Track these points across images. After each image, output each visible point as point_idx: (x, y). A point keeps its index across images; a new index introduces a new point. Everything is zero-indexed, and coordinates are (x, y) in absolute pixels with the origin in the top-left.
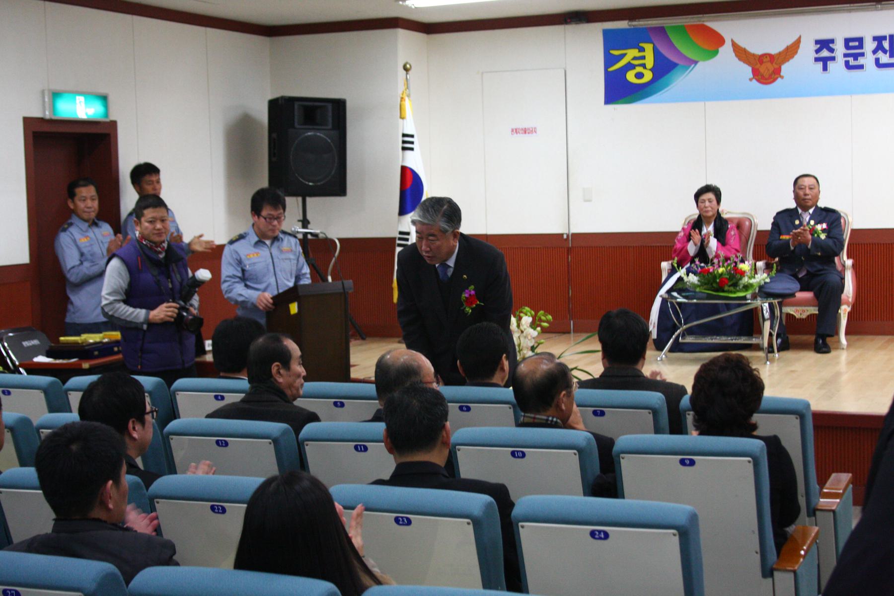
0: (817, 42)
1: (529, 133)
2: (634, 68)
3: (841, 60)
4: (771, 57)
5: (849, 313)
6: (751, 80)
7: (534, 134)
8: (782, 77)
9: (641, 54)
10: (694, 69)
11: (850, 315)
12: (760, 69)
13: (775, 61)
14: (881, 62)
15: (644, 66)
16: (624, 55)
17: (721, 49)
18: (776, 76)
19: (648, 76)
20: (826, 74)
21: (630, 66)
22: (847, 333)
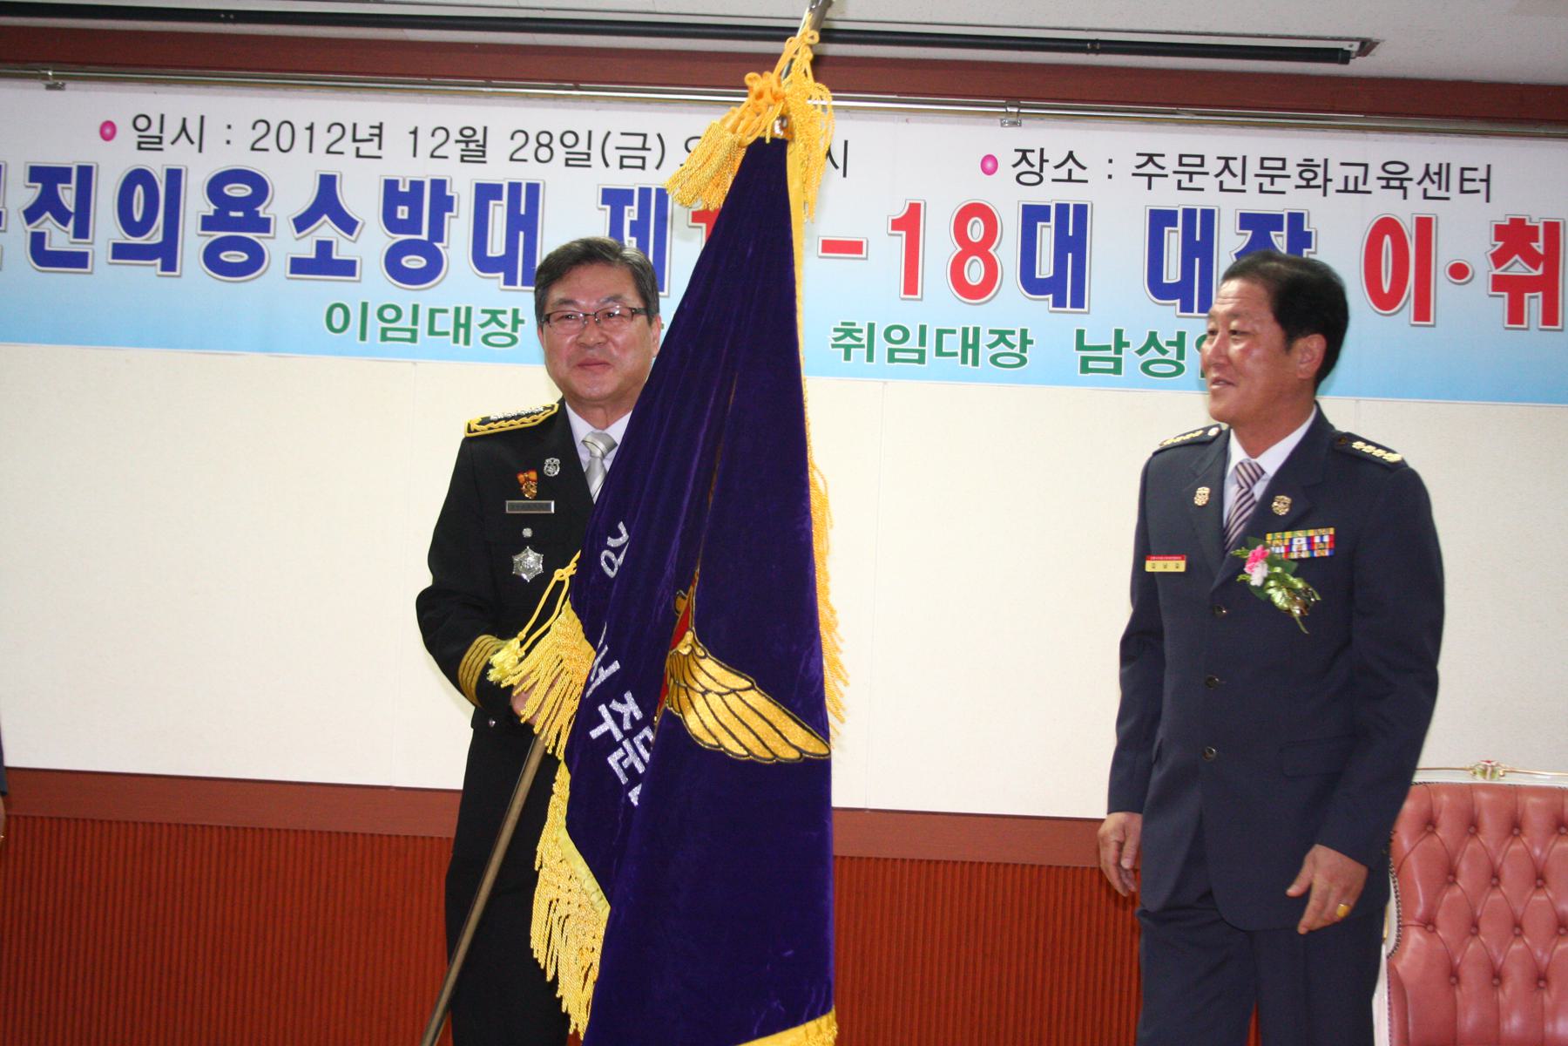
14: (47, 248)
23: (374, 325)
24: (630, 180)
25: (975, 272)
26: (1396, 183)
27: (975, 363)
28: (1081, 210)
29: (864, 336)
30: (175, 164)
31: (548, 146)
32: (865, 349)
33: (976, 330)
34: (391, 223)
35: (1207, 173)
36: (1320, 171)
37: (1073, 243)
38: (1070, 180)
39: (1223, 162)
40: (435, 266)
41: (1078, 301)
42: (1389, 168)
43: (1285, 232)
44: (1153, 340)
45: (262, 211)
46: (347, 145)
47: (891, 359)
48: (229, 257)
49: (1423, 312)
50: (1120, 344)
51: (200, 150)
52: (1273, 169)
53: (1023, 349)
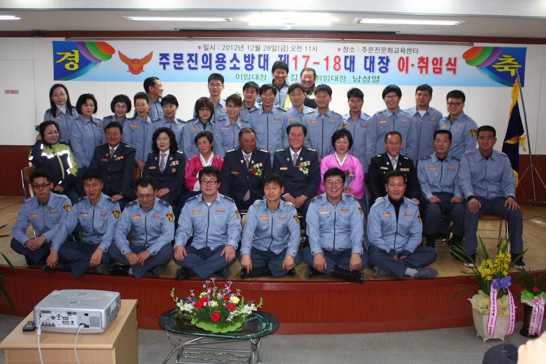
0: (161, 55)
1: (14, 93)
2: (69, 63)
3: (172, 65)
4: (138, 61)
6: (128, 72)
7: (18, 94)
8: (144, 71)
9: (73, 55)
10: (100, 64)
12: (133, 67)
14: (191, 67)
15: (74, 61)
16: (65, 55)
17: (113, 55)
18: (141, 70)
19: (76, 67)
20: (164, 71)
21: (67, 61)
23: (243, 77)
24: (283, 53)
25: (337, 66)
28: (354, 57)
32: (320, 80)
34: (245, 61)
36: (391, 50)
37: (352, 62)
38: (352, 52)
39: (376, 49)
40: (252, 68)
41: (353, 71)
44: (365, 77)
45: (225, 60)
46: (238, 49)
48: (220, 67)
49: (407, 72)
50: (360, 78)
52: (384, 49)
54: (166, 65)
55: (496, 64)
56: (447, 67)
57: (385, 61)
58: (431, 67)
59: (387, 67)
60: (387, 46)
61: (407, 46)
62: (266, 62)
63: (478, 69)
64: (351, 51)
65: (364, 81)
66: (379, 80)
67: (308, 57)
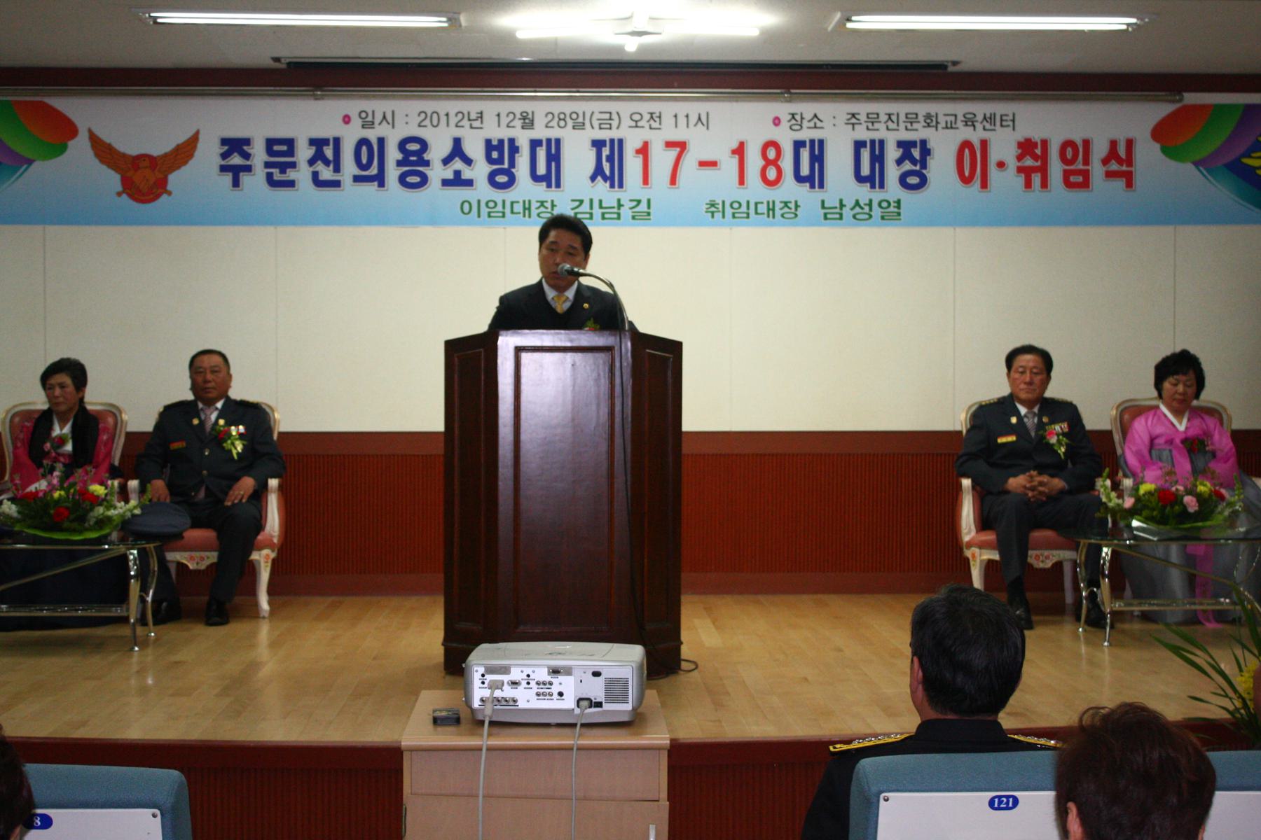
0: (224, 141)
3: (260, 172)
5: (274, 560)
6: (119, 194)
8: (169, 193)
11: (276, 566)
13: (158, 167)
20: (236, 193)
22: (271, 591)
23: (484, 210)
25: (771, 174)
26: (970, 123)
27: (774, 217)
28: (821, 142)
29: (720, 207)
30: (381, 135)
31: (564, 120)
32: (721, 214)
33: (774, 202)
34: (490, 160)
35: (880, 122)
36: (934, 119)
37: (818, 158)
38: (815, 127)
39: (887, 117)
40: (512, 181)
41: (821, 186)
42: (968, 116)
43: (918, 149)
44: (857, 203)
45: (426, 157)
46: (466, 123)
47: (734, 217)
49: (984, 185)
50: (842, 205)
51: (393, 127)
52: (911, 119)
53: (796, 210)
54: (241, 174)
55: (1254, 155)
56: (1104, 169)
57: (916, 153)
58: (1056, 168)
59: (924, 171)
60: (922, 108)
61: (981, 109)
62: (553, 164)
63: (1201, 172)
64: (812, 124)
65: (854, 217)
66: (901, 211)
67: (682, 146)
